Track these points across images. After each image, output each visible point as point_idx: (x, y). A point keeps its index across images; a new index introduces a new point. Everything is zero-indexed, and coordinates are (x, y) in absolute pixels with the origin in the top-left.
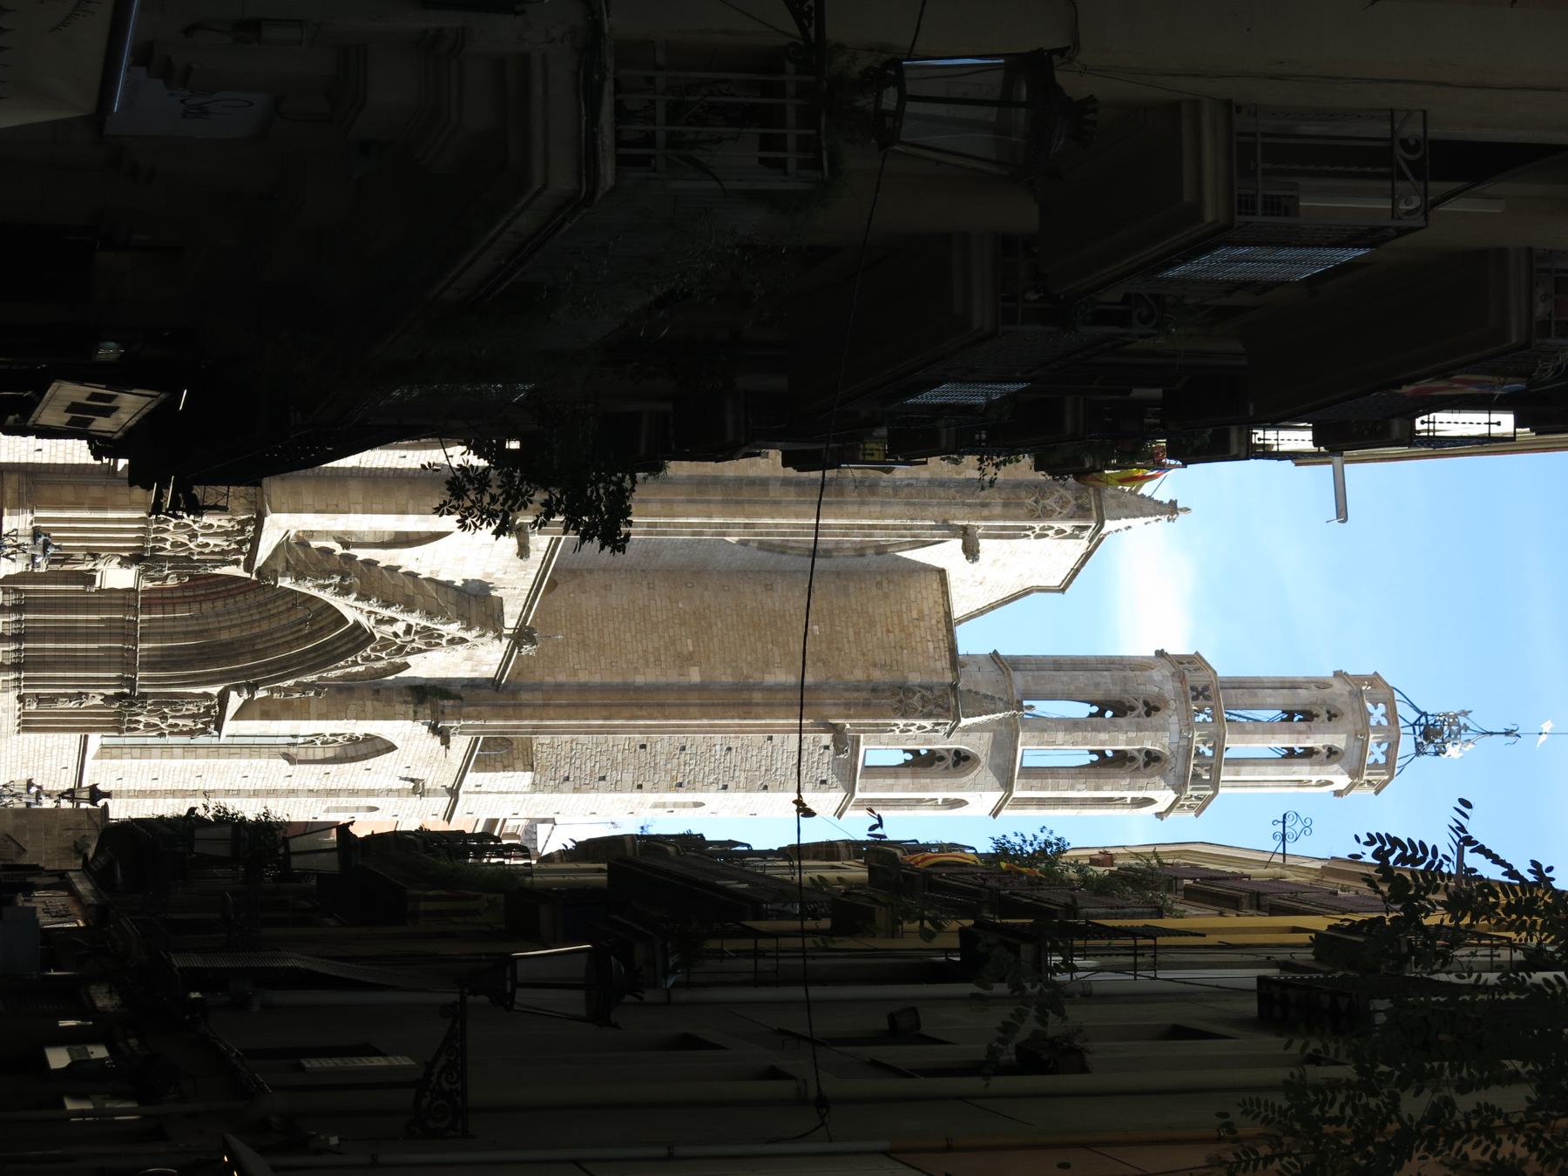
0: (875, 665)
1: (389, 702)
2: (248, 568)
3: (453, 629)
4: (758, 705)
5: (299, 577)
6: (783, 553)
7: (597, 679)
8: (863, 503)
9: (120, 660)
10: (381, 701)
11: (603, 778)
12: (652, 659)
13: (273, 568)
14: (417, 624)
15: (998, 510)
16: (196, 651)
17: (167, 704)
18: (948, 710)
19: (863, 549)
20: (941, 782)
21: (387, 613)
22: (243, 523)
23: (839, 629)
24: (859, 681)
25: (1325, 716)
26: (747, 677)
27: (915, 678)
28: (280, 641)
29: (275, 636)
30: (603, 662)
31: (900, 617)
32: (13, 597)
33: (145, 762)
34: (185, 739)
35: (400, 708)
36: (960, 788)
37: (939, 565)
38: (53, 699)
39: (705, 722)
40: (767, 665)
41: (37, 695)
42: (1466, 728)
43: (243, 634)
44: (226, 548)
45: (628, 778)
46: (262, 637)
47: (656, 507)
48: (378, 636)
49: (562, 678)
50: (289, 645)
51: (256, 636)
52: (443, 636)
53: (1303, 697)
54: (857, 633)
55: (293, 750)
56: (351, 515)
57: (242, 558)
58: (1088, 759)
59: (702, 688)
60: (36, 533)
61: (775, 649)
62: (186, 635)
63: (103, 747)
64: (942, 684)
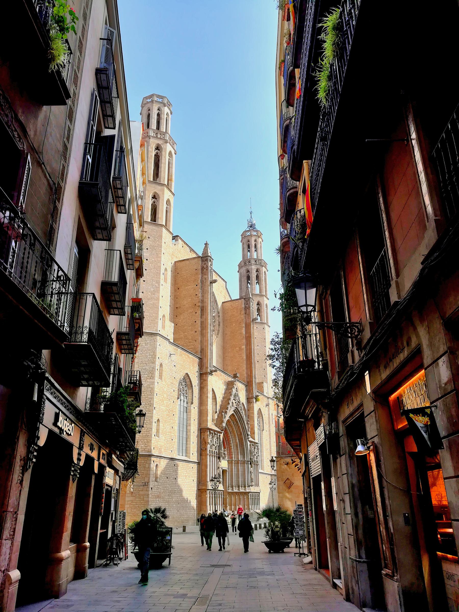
1: (250, 408)
2: (221, 433)
3: (234, 390)
5: (223, 422)
8: (206, 303)
17: (252, 454)
20: (262, 307)
27: (243, 306)
31: (232, 309)
33: (265, 460)
34: (259, 450)
36: (264, 304)
42: (250, 220)
47: (206, 343)
48: (236, 407)
50: (239, 427)
53: (246, 247)
57: (218, 434)
58: (258, 285)
60: (212, 480)
62: (237, 449)
63: (262, 469)
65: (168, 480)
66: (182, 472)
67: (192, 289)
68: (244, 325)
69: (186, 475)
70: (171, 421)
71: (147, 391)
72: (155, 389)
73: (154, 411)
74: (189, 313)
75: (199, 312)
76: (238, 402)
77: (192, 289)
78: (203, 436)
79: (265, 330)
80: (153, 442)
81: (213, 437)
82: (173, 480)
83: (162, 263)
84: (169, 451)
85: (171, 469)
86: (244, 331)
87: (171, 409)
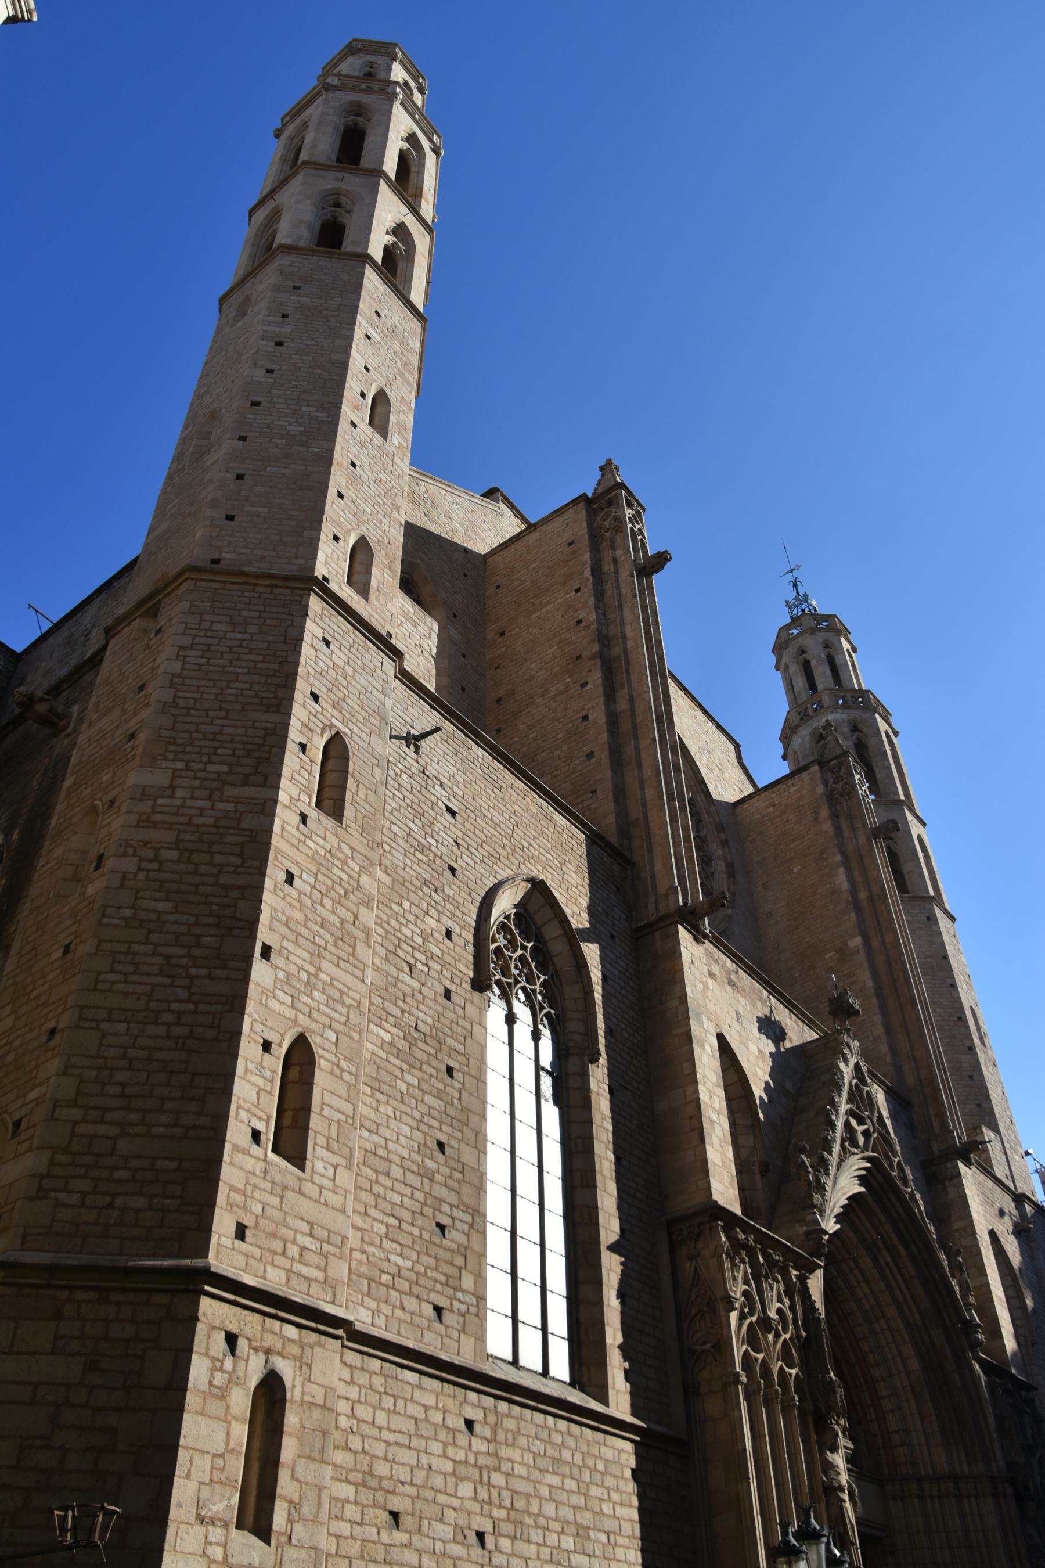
0: (816, 819)
2: (812, 1268)
11: (971, 1077)
12: (850, 980)
15: (619, 552)
21: (840, 1124)
22: (737, 1246)
25: (805, 655)
27: (820, 789)
28: (906, 1292)
29: (901, 1299)
35: (952, 1193)
43: (908, 1340)
44: (782, 1288)
45: (964, 1058)
49: (884, 1048)
52: (856, 1084)
54: (794, 841)
56: (701, 1097)
64: (821, 773)
65: (400, 1537)
66: (545, 1491)
67: (558, 610)
68: (838, 858)
69: (586, 1518)
70: (428, 1098)
71: (216, 848)
72: (275, 840)
73: (260, 972)
74: (553, 698)
75: (596, 677)
76: (880, 1133)
77: (558, 610)
78: (688, 1266)
79: (937, 924)
80: (229, 1174)
81: (757, 1278)
82: (457, 1550)
83: (358, 357)
84: (411, 1303)
85: (436, 1447)
86: (841, 879)
87: (421, 1025)
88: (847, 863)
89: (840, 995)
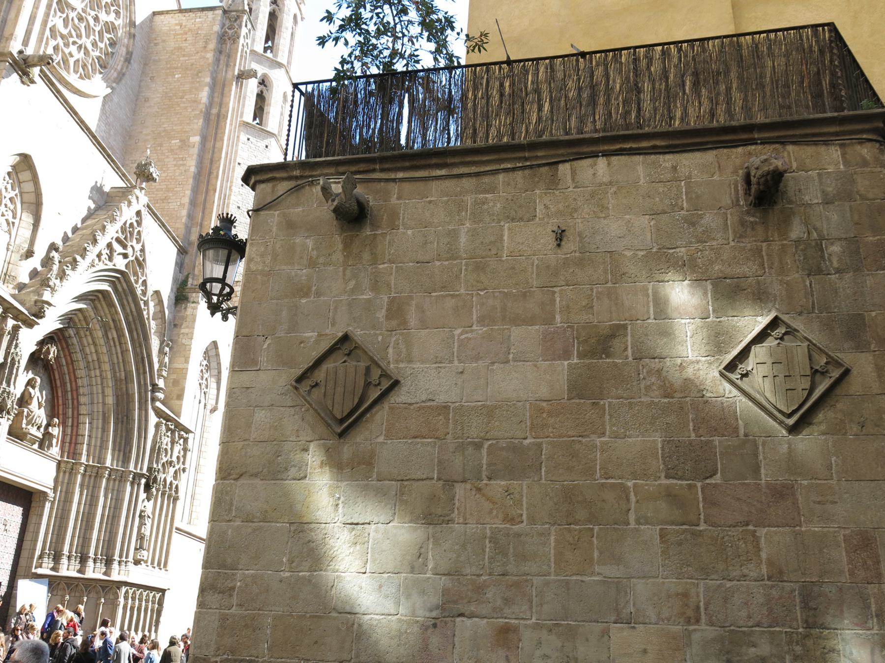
0: (205, 47)
1: (184, 318)
4: (220, 111)
6: (124, 75)
7: (188, 193)
9: (117, 482)
10: (182, 324)
12: (181, 162)
13: (33, 303)
14: (117, 232)
16: (120, 425)
18: (238, 17)
19: (130, 34)
23: (179, 65)
24: (214, 55)
26: (201, 111)
27: (217, 28)
30: (179, 189)
31: (178, 35)
32: (46, 560)
35: (189, 311)
37: (150, 12)
38: (141, 537)
39: (226, 138)
40: (196, 101)
41: (136, 549)
43: (110, 385)
46: (115, 372)
48: (123, 268)
49: (184, 212)
50: (124, 352)
51: (114, 376)
52: (131, 225)
54: (184, 56)
55: (209, 407)
59: (204, 139)
61: (186, 97)
62: (105, 430)
68: (208, 80)
76: (137, 258)
86: (204, 95)
88: (213, 87)
89: (146, 164)
